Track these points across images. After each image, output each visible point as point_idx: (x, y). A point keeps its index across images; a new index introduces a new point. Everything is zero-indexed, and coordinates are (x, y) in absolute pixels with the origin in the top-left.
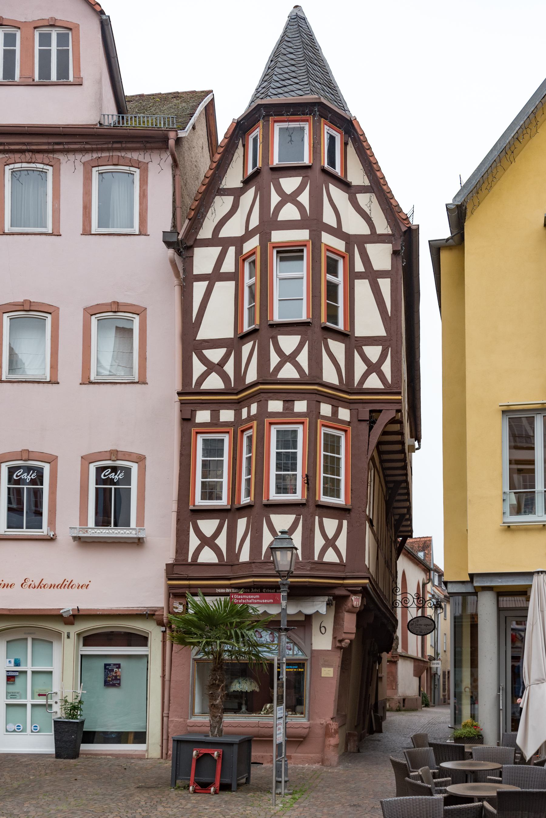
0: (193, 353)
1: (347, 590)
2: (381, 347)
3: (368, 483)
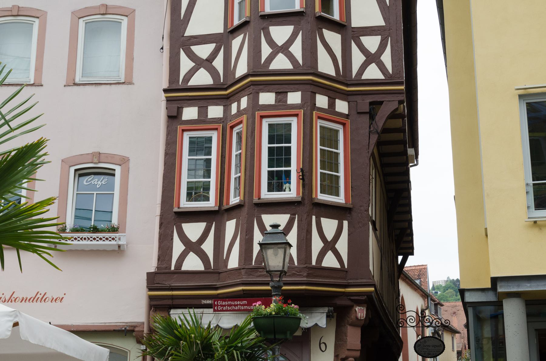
0: (181, 49)
1: (350, 299)
2: (380, 37)
3: (370, 180)
